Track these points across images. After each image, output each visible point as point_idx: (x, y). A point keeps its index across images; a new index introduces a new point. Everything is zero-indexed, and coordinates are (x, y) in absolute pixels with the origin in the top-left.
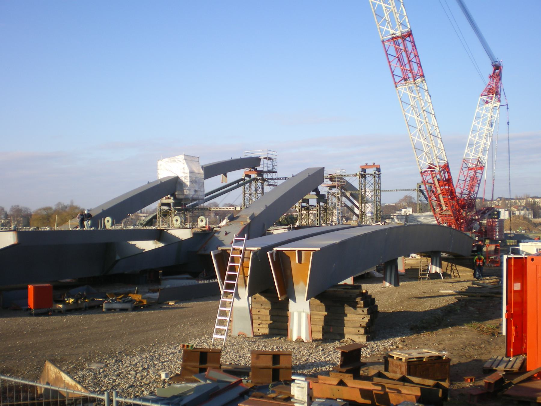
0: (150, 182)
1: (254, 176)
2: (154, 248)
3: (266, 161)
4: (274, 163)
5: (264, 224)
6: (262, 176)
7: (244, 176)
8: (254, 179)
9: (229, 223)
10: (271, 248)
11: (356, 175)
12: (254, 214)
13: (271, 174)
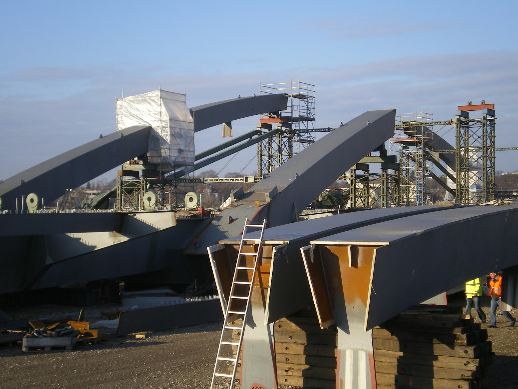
0: (103, 136)
1: (276, 126)
2: (111, 244)
3: (296, 101)
4: (310, 104)
5: (293, 204)
6: (290, 126)
7: (261, 126)
8: (277, 131)
9: (235, 204)
10: (305, 241)
11: (450, 123)
12: (276, 187)
13: (306, 123)
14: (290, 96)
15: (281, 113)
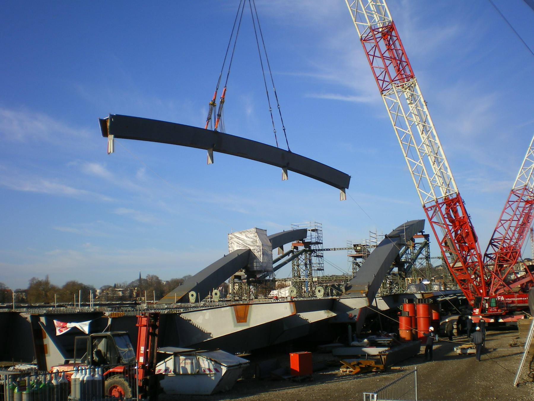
1: (301, 248)
4: (319, 234)
6: (310, 248)
7: (293, 248)
8: (304, 251)
14: (309, 230)
15: (305, 240)
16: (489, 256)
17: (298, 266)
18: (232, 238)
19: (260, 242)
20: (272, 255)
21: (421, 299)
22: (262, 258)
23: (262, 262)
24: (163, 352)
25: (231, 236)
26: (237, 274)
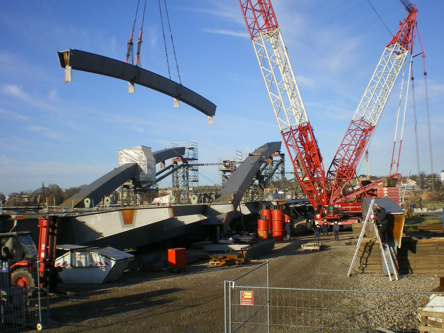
1: (180, 163)
4: (195, 152)
8: (182, 165)
14: (187, 148)
16: (332, 172)
17: (177, 178)
18: (121, 154)
19: (146, 157)
20: (155, 168)
21: (276, 206)
22: (148, 171)
23: (147, 174)
24: (61, 249)
25: (120, 152)
26: (126, 184)
